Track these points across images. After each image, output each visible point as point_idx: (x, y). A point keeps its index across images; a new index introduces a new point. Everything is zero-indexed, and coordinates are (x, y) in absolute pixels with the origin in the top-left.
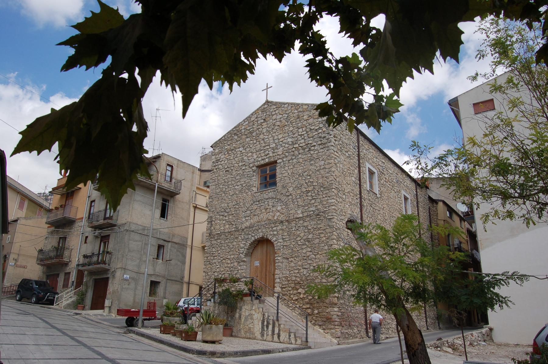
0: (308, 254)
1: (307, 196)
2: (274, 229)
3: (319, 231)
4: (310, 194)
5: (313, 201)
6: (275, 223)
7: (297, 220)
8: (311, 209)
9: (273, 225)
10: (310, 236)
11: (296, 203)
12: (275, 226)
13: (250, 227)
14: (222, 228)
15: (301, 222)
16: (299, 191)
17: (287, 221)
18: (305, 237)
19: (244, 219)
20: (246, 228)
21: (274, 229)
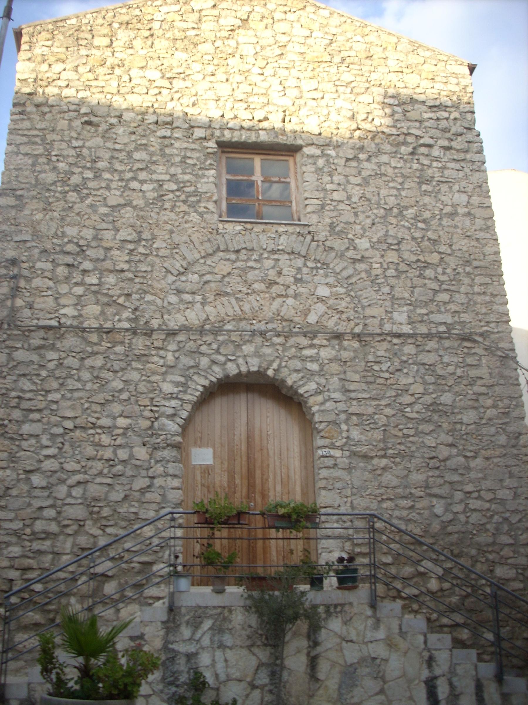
0: (444, 452)
1: (420, 276)
2: (307, 352)
3: (476, 389)
4: (429, 273)
5: (444, 297)
6: (311, 333)
7: (395, 341)
8: (437, 318)
9: (305, 342)
10: (447, 398)
11: (386, 290)
12: (312, 346)
13: (201, 331)
14: (70, 311)
15: (409, 349)
16: (392, 257)
17: (358, 337)
18: (428, 399)
19: (173, 299)
20: (185, 328)
21: (307, 352)
